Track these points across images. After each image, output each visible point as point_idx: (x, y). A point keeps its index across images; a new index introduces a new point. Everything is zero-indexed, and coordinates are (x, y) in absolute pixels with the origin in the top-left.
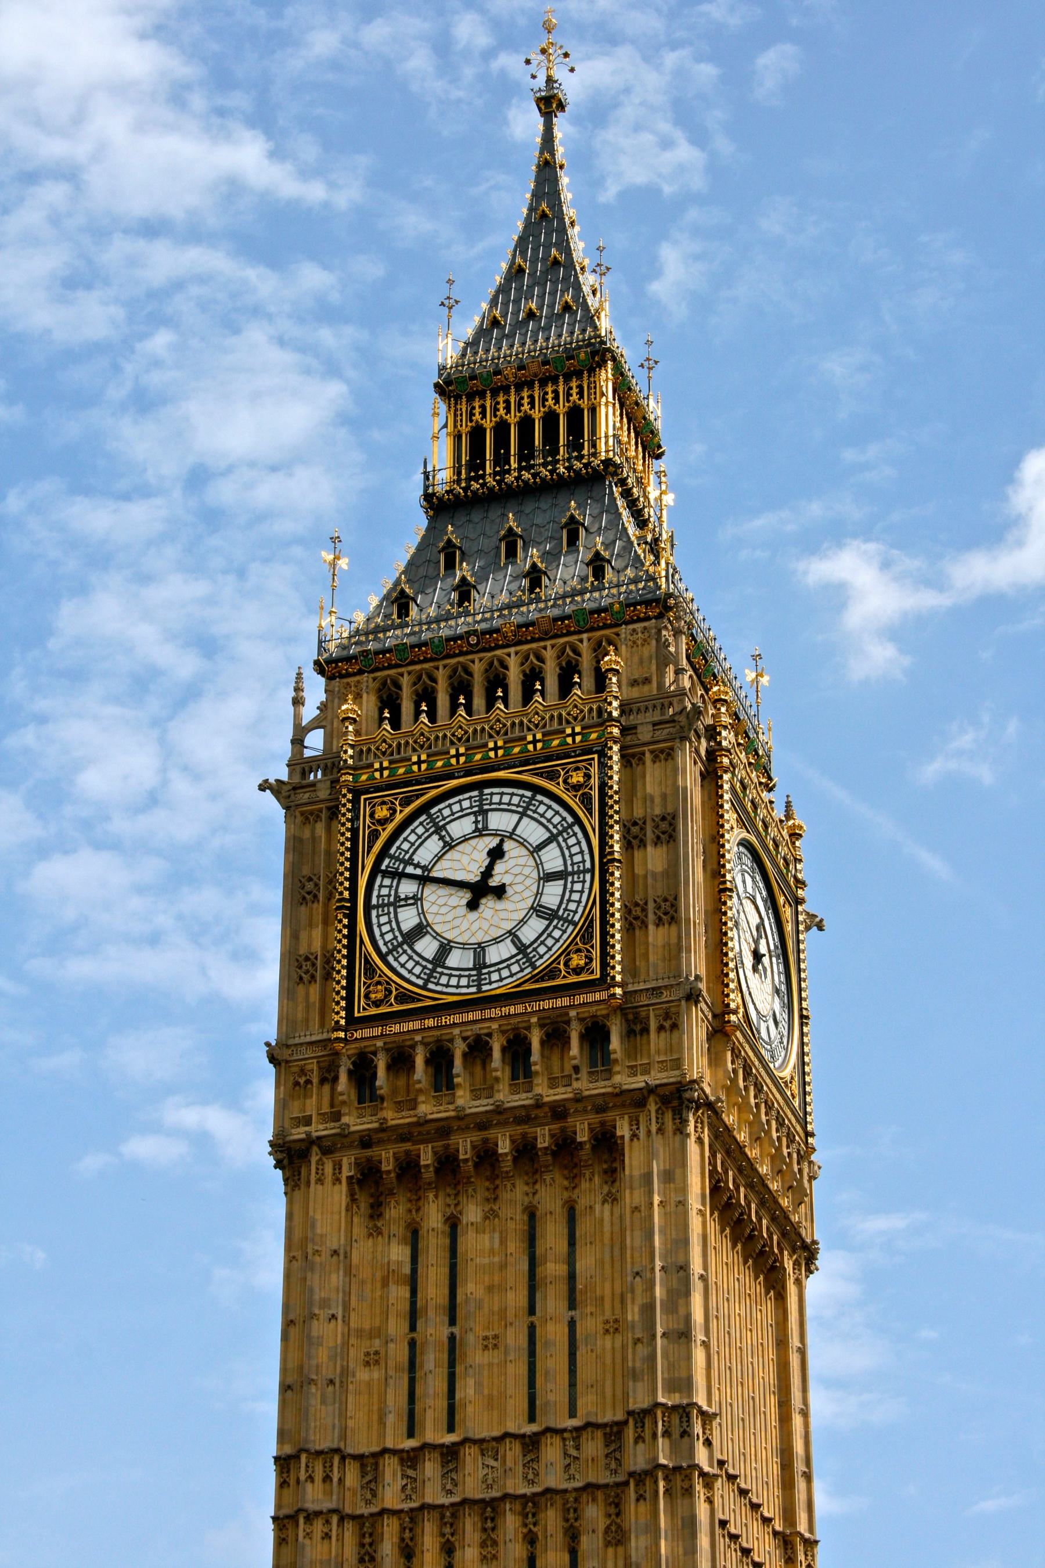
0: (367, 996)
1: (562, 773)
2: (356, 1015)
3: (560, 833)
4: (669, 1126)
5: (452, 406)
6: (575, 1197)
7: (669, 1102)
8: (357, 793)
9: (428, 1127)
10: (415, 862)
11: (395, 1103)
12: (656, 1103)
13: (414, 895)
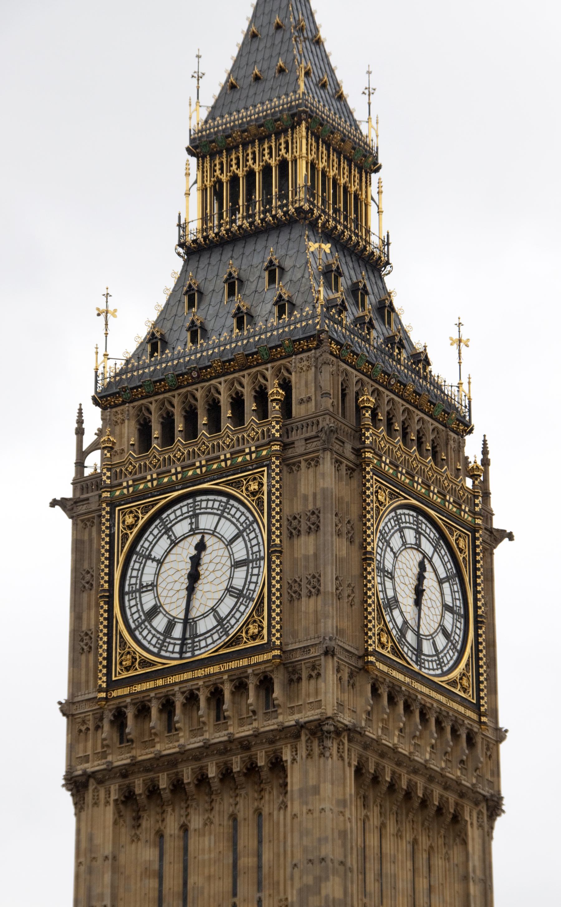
0: (121, 663)
1: (245, 483)
2: (114, 679)
3: (245, 530)
4: (316, 750)
5: (200, 164)
6: (261, 806)
10: (153, 557)
11: (143, 742)
12: (306, 735)
13: (152, 583)
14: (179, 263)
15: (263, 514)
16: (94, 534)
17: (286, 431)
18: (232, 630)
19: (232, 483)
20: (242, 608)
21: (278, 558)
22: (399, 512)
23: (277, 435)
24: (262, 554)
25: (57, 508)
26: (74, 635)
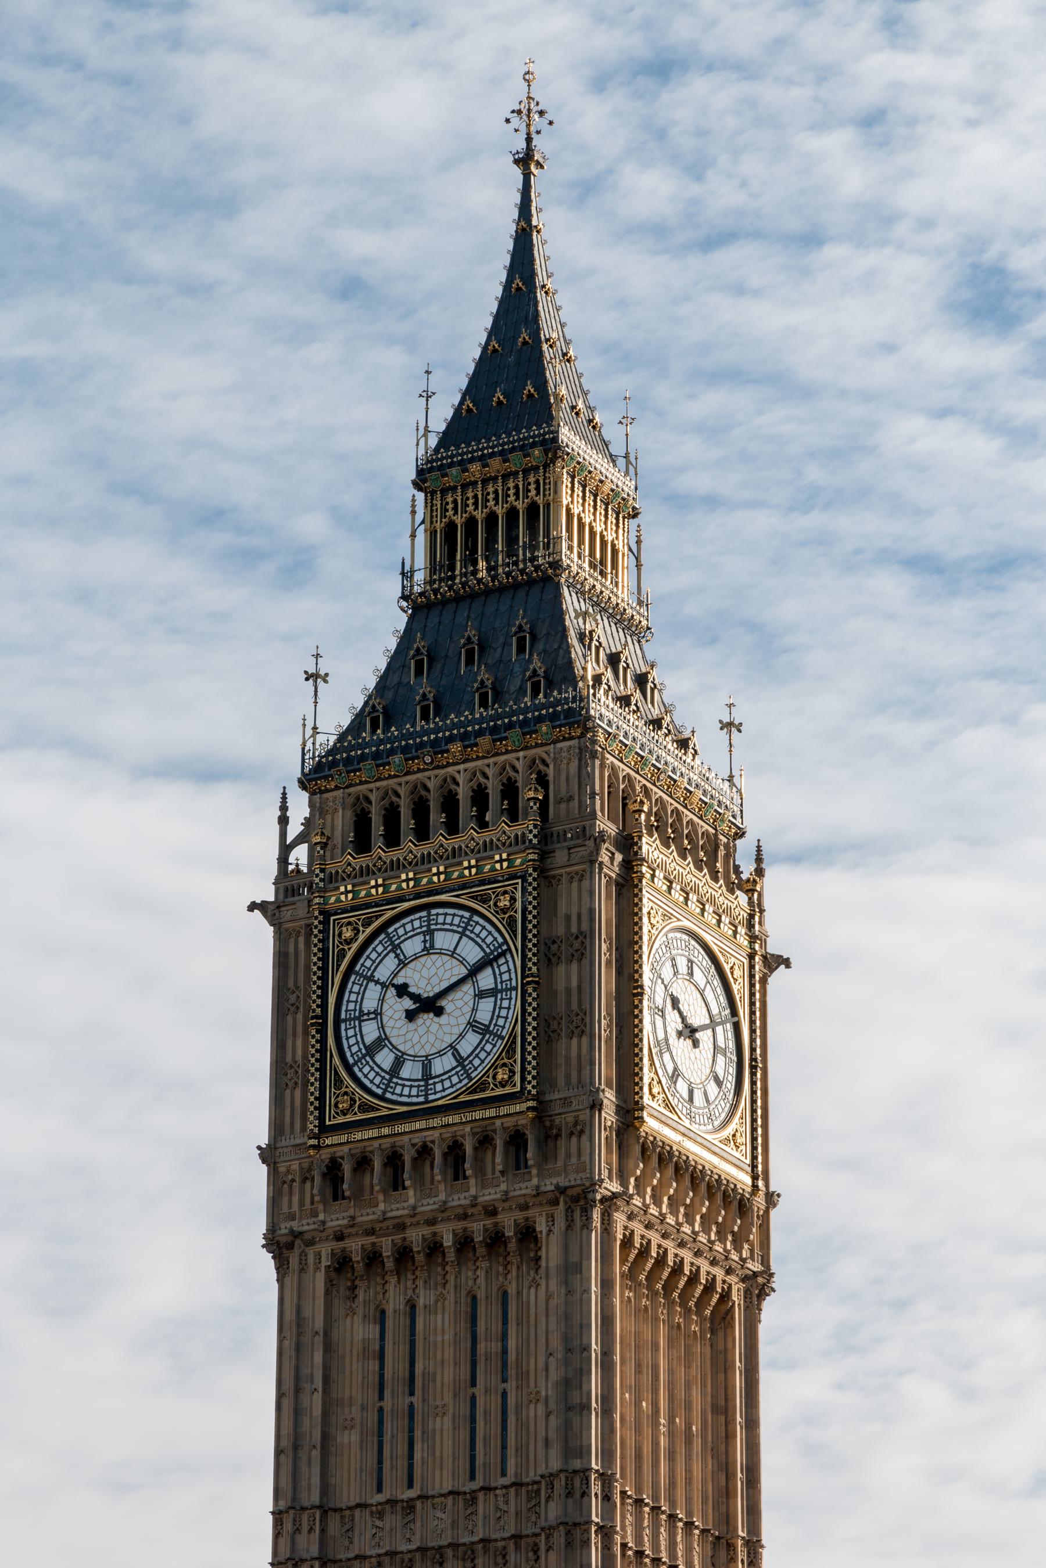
2: (328, 1123)
5: (429, 501)
7: (578, 1201)
8: (326, 914)
10: (376, 979)
12: (566, 1203)
14: (401, 621)
16: (302, 946)
17: (545, 837)
19: (477, 896)
22: (670, 935)
23: (535, 841)
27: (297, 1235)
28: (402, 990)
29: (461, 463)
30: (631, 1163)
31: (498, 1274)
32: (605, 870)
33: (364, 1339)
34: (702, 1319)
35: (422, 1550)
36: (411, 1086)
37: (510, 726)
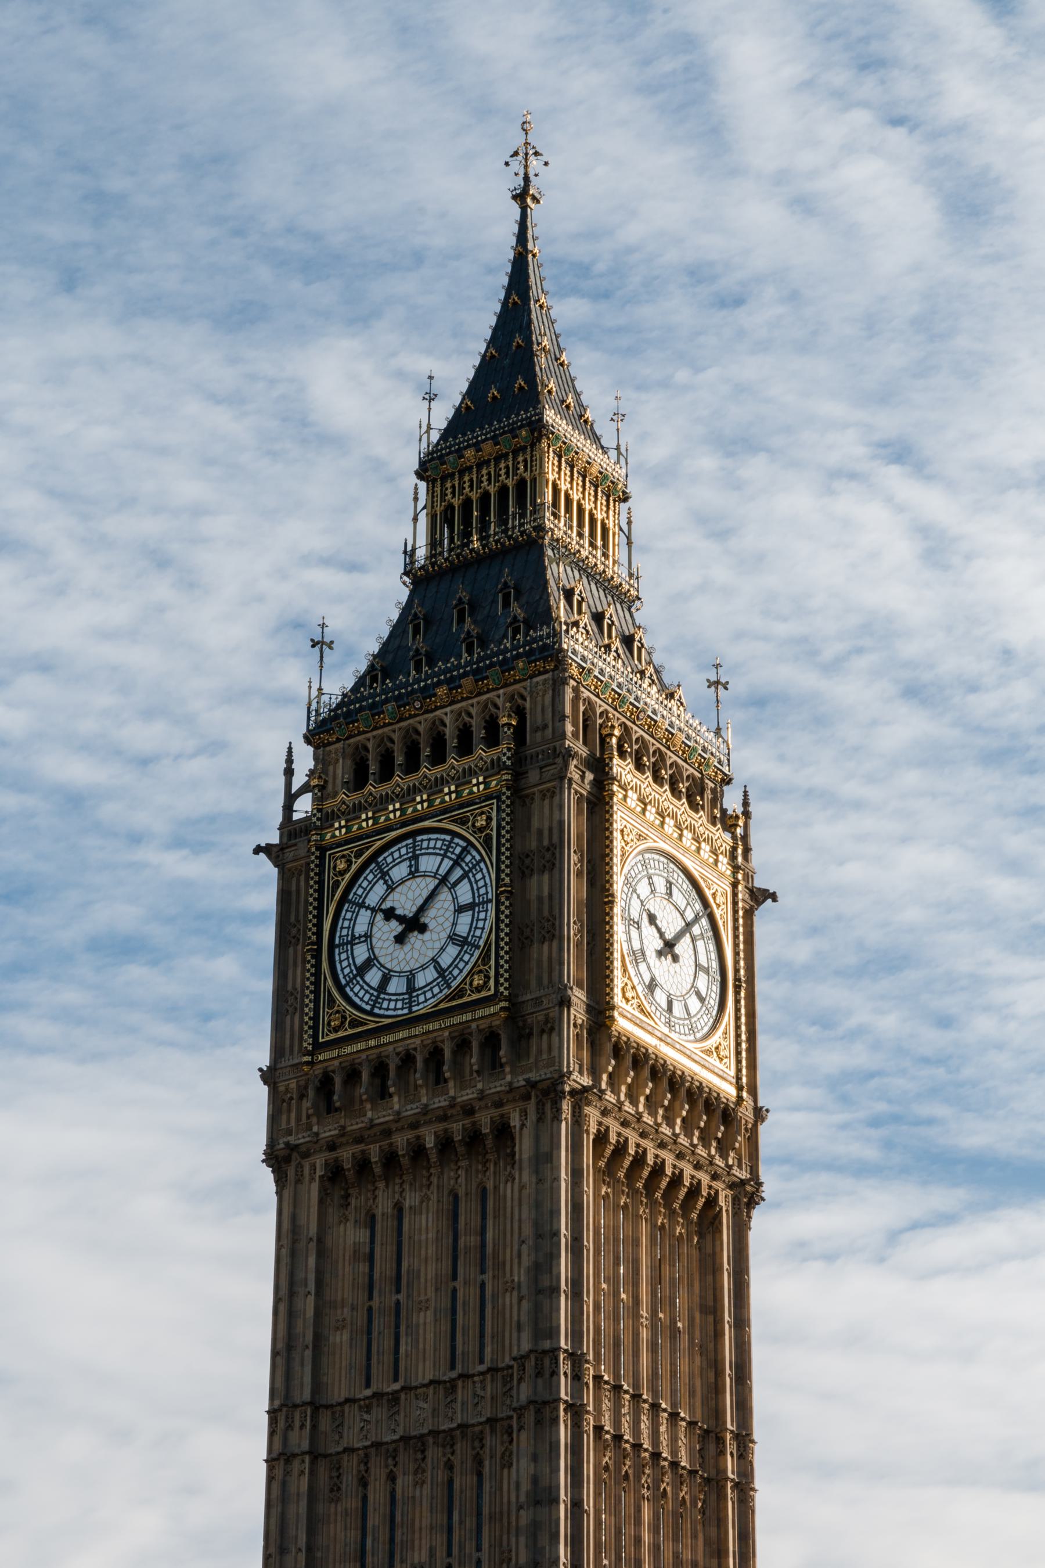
2: (321, 1040)
3: (470, 870)
5: (430, 488)
8: (322, 849)
9: (376, 1130)
12: (537, 1096)
15: (491, 852)
16: (302, 884)
18: (455, 982)
20: (466, 957)
21: (507, 899)
22: (647, 856)
23: (509, 763)
24: (490, 896)
25: (262, 855)
26: (278, 995)
27: (292, 1148)
28: (390, 914)
29: (458, 451)
30: (603, 1061)
31: (477, 1171)
32: (574, 786)
33: (354, 1243)
34: (689, 1222)
35: (405, 1439)
36: (397, 1000)
37: (492, 665)
